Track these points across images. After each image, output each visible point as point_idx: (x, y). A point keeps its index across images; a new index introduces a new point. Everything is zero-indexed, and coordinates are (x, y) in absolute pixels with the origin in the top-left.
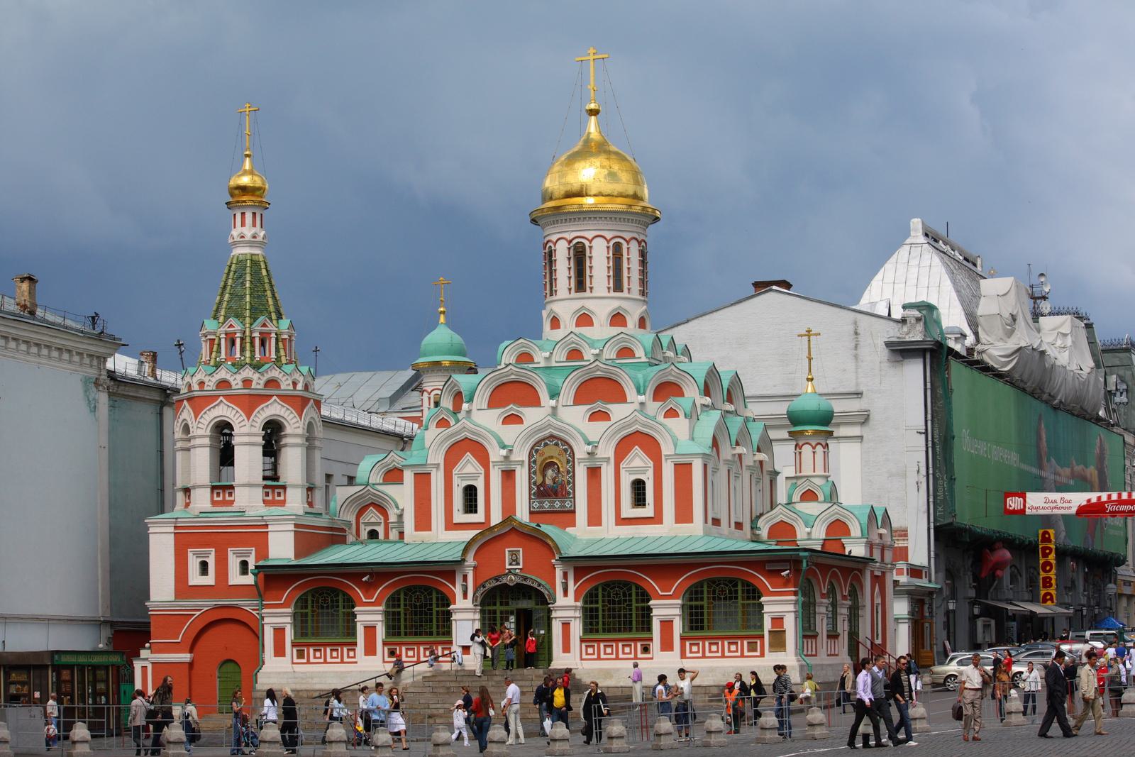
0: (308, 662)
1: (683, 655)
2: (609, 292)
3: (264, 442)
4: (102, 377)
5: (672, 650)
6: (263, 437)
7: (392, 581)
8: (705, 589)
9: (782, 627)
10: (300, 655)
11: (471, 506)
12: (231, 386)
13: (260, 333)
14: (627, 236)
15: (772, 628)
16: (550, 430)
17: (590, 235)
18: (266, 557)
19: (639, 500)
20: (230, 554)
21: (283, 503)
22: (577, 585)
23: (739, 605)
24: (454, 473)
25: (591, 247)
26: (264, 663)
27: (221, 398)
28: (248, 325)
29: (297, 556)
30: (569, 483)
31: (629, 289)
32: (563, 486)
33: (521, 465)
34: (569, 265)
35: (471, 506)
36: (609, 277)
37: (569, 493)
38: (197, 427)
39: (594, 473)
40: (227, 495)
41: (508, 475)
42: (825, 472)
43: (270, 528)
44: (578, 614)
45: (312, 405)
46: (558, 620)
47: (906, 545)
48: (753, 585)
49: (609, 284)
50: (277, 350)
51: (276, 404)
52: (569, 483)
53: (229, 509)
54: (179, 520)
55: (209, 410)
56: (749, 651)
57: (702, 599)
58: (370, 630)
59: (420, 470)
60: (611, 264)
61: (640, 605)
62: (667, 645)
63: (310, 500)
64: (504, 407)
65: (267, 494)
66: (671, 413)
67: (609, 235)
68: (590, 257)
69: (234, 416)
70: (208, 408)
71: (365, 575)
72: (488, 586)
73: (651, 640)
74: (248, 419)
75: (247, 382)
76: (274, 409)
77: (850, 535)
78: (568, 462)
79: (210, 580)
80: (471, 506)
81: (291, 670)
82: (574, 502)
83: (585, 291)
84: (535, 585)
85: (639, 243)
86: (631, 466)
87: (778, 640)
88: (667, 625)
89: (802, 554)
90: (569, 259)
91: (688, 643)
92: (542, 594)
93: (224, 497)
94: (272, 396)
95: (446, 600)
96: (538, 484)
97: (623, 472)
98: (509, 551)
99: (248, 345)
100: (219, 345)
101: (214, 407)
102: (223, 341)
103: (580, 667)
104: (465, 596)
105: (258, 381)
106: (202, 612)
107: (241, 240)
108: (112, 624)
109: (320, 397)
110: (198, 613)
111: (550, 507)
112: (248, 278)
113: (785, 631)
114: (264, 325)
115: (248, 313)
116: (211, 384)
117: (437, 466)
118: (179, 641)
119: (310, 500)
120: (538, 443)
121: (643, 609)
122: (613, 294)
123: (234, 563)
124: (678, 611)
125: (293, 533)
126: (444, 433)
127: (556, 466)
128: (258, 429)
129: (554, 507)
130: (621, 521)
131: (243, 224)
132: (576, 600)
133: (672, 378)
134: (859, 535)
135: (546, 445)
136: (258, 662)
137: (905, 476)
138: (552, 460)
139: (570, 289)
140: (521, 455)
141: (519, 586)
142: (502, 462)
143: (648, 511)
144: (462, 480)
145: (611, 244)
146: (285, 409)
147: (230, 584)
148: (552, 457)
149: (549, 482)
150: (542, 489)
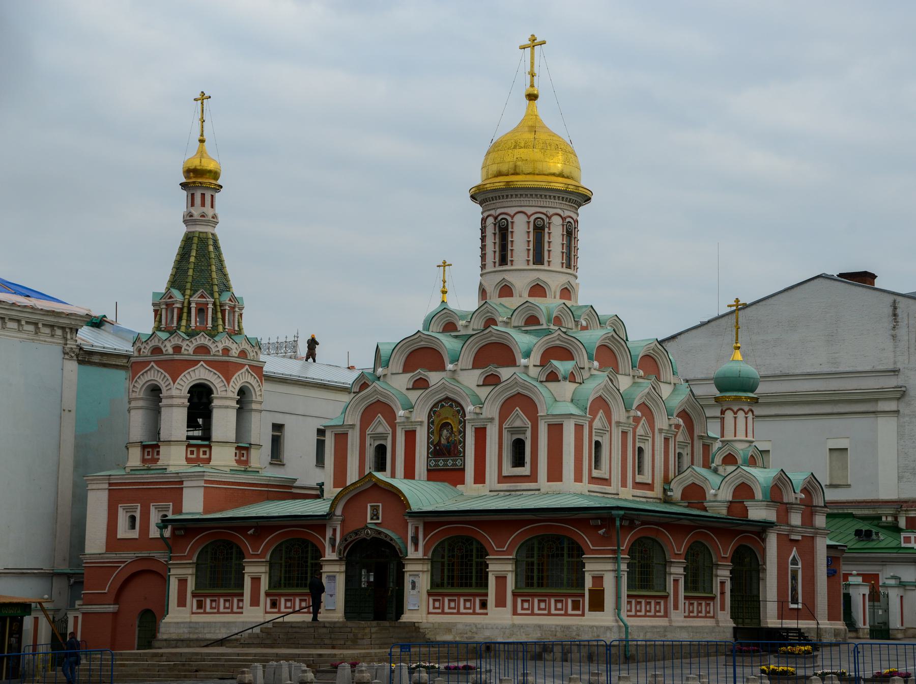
0: (205, 613)
1: (515, 613)
2: (528, 264)
3: (189, 404)
4: (68, 346)
5: (505, 606)
6: (188, 400)
7: (273, 535)
8: (536, 546)
9: (602, 586)
10: (200, 605)
12: (162, 351)
13: (196, 304)
14: (551, 211)
15: (593, 587)
16: (446, 392)
17: (512, 211)
18: (180, 513)
19: (518, 460)
20: (152, 509)
21: (209, 460)
22: (425, 542)
23: (565, 562)
24: (367, 433)
25: (512, 223)
26: (168, 614)
27: (152, 363)
28: (187, 297)
29: (206, 511)
30: (460, 442)
31: (549, 262)
32: (455, 444)
33: (420, 425)
34: (495, 240)
36: (529, 250)
37: (460, 452)
38: (133, 391)
39: (481, 433)
40: (155, 454)
43: (185, 484)
44: (427, 567)
45: (247, 369)
46: (408, 573)
48: (577, 544)
49: (528, 257)
50: (214, 319)
51: (202, 370)
52: (460, 442)
53: (153, 466)
54: (112, 477)
55: (143, 374)
56: (573, 609)
57: (533, 557)
58: (256, 580)
59: (339, 430)
60: (531, 238)
61: (479, 560)
62: (500, 603)
63: (244, 458)
64: (413, 372)
65: (192, 453)
66: (553, 377)
67: (530, 211)
68: (512, 232)
69: (162, 381)
70: (141, 373)
71: (249, 528)
72: (350, 540)
73: (486, 595)
74: (174, 383)
75: (177, 349)
76: (201, 374)
77: (754, 498)
78: (460, 422)
79: (135, 534)
81: (188, 620)
82: (464, 459)
83: (507, 264)
84: (388, 540)
85: (563, 219)
86: (513, 426)
87: (597, 603)
88: (501, 580)
89: (614, 512)
90: (495, 234)
91: (519, 600)
92: (394, 547)
93: (153, 455)
94: (200, 361)
95: (318, 553)
96: (435, 443)
97: (505, 433)
98: (371, 506)
99: (185, 315)
100: (161, 315)
101: (146, 372)
102: (164, 312)
103: (425, 621)
104: (333, 551)
105: (188, 348)
106: (125, 564)
107: (201, 218)
108: (68, 576)
109: (263, 364)
110: (123, 565)
111: (444, 465)
112: (194, 253)
113: (603, 590)
114: (202, 296)
115: (188, 286)
116: (146, 351)
117: (352, 426)
118: (106, 591)
119: (244, 458)
120: (435, 405)
121: (481, 563)
123: (155, 517)
124: (510, 567)
125: (203, 489)
126: (356, 398)
127: (450, 427)
128: (185, 392)
129: (447, 465)
130: (502, 479)
131: (193, 205)
132: (425, 554)
135: (443, 406)
136: (165, 611)
138: (447, 421)
140: (421, 415)
141: (374, 539)
142: (404, 422)
143: (525, 470)
146: (212, 373)
147: (150, 537)
148: (447, 418)
149: (443, 441)
150: (438, 448)
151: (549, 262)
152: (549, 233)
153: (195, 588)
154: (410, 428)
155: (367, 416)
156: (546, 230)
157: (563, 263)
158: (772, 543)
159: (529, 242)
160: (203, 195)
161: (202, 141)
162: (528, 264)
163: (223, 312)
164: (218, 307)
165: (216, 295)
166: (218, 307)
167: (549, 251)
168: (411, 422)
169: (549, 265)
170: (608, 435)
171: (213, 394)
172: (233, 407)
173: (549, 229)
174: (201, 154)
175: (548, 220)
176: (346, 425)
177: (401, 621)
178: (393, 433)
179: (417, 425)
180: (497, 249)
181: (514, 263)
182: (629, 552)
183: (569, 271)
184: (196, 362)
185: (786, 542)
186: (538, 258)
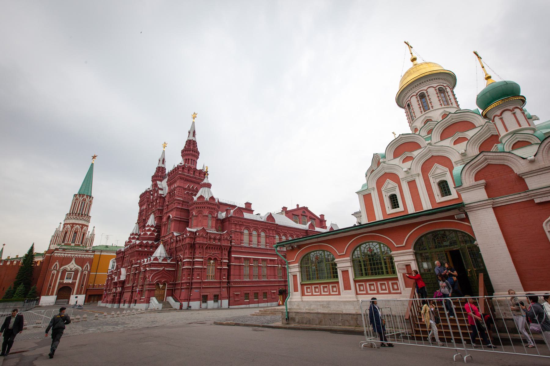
11: (395, 205)
14: (445, 85)
17: (425, 88)
24: (382, 190)
25: (427, 92)
33: (418, 176)
35: (395, 204)
41: (412, 184)
67: (435, 85)
68: (428, 96)
80: (395, 205)
90: (418, 101)
122: (443, 106)
139: (421, 112)
142: (406, 177)
144: (387, 193)
145: (437, 88)
151: (452, 104)
154: (410, 179)
155: (380, 183)
162: (442, 106)
168: (412, 176)
169: (452, 105)
175: (445, 88)
176: (369, 189)
178: (399, 186)
179: (416, 176)
180: (421, 105)
181: (433, 107)
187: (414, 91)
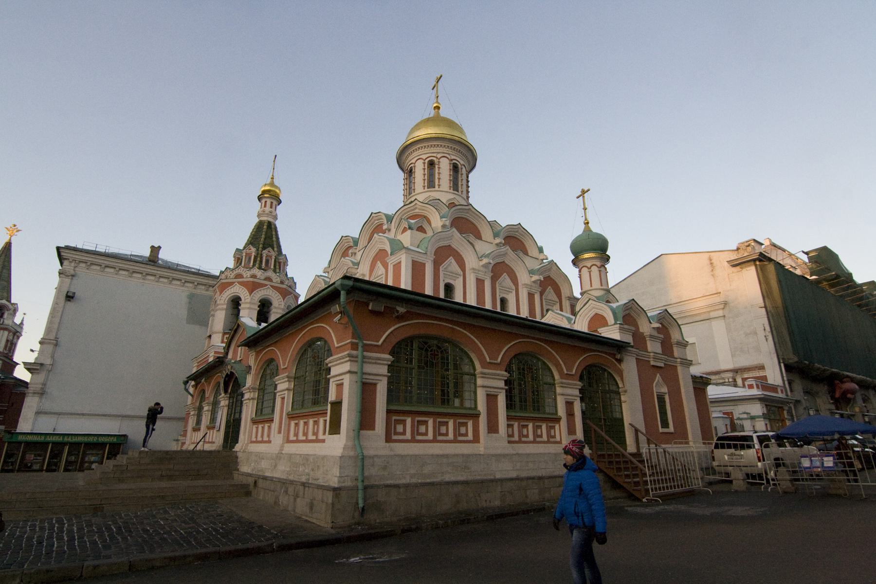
13: (246, 254)
14: (439, 156)
17: (413, 161)
25: (415, 166)
31: (439, 185)
36: (424, 180)
42: (601, 285)
47: (765, 375)
50: (255, 261)
60: (426, 173)
67: (424, 157)
91: (293, 423)
122: (426, 189)
133: (420, 211)
134: (613, 322)
137: (756, 333)
145: (426, 161)
151: (439, 185)
152: (439, 168)
153: (196, 425)
156: (437, 166)
157: (450, 187)
158: (629, 368)
159: (424, 175)
160: (266, 202)
161: (272, 178)
162: (424, 189)
163: (261, 258)
164: (259, 255)
165: (260, 249)
166: (259, 255)
167: (439, 179)
170: (461, 279)
171: (241, 300)
172: (255, 309)
173: (439, 165)
174: (272, 184)
177: (233, 450)
182: (390, 352)
183: (456, 192)
184: (232, 284)
185: (646, 370)
186: (431, 183)
187: (450, 152)
